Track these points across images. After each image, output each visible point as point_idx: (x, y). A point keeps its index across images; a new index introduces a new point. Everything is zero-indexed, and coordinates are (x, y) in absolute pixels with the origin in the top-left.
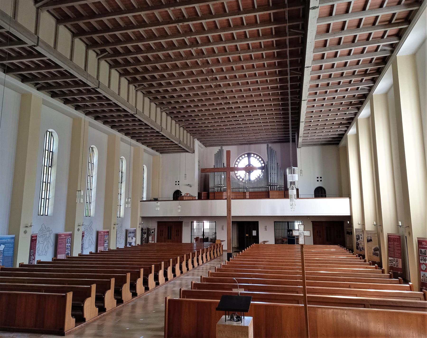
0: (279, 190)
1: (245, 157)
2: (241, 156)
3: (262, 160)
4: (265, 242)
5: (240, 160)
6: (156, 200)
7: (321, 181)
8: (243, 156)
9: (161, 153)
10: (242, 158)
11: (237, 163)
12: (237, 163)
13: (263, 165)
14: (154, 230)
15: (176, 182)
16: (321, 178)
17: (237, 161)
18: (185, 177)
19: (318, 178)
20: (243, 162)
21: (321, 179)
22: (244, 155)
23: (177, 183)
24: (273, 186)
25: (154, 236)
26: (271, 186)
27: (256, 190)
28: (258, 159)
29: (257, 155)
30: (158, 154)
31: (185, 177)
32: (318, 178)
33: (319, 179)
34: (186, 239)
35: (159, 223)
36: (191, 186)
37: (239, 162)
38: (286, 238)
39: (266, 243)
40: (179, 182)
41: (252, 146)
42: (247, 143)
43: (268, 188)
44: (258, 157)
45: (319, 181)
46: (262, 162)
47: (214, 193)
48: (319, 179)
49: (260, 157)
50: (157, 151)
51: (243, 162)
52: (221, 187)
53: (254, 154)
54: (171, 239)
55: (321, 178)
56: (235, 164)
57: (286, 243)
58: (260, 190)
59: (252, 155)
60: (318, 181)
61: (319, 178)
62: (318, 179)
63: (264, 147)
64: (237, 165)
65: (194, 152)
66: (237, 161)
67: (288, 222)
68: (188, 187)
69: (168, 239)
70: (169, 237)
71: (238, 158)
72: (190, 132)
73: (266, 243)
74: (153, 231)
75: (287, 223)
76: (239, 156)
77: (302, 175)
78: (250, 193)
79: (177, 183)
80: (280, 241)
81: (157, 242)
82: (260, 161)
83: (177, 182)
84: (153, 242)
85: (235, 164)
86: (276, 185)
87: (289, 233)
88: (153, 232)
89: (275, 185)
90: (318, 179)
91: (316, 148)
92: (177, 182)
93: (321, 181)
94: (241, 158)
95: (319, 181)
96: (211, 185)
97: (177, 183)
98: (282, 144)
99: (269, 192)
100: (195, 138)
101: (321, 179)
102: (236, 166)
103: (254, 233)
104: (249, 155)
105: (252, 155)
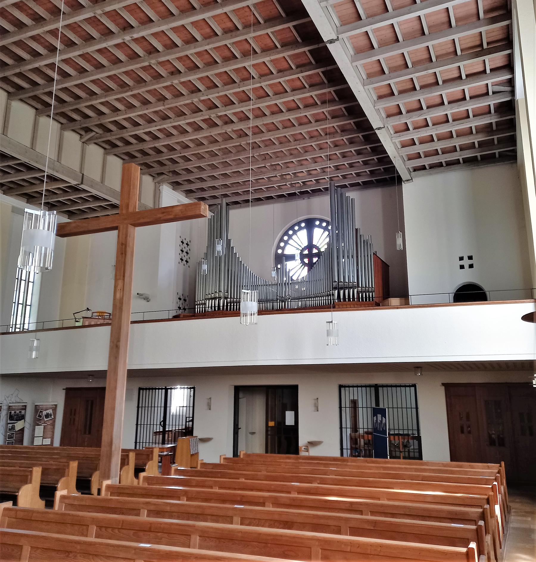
4: (312, 444)
7: (471, 266)
16: (470, 258)
21: (470, 262)
25: (53, 425)
32: (461, 259)
33: (466, 262)
35: (70, 393)
36: (147, 299)
45: (466, 266)
48: (466, 262)
60: (462, 267)
61: (466, 258)
62: (462, 263)
67: (376, 387)
74: (50, 411)
75: (373, 389)
84: (47, 442)
88: (47, 416)
90: (462, 263)
93: (471, 266)
95: (466, 266)
101: (470, 262)
103: (289, 419)
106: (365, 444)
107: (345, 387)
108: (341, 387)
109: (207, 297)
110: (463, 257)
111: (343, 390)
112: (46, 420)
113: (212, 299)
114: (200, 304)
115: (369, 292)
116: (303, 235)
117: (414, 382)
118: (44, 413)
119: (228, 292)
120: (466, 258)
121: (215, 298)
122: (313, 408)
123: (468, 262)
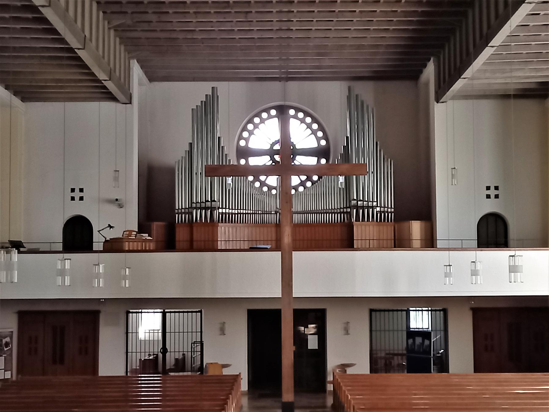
0: (381, 219)
1: (270, 117)
2: (258, 115)
3: (321, 128)
4: (343, 367)
5: (256, 126)
6: (17, 245)
7: (497, 196)
8: (264, 115)
9: (23, 100)
10: (262, 121)
11: (245, 134)
12: (245, 134)
13: (323, 143)
14: (11, 338)
15: (73, 190)
16: (496, 188)
17: (245, 129)
18: (116, 179)
19: (488, 188)
20: (264, 134)
21: (496, 192)
22: (267, 110)
23: (77, 194)
24: (363, 207)
25: (11, 355)
26: (357, 207)
27: (311, 218)
28: (309, 126)
29: (307, 114)
30: (16, 101)
31: (116, 179)
32: (488, 188)
33: (492, 192)
34: (111, 363)
36: (121, 206)
37: (251, 133)
38: (402, 355)
39: (349, 371)
40: (81, 190)
41: (292, 85)
42: (280, 76)
43: (350, 214)
44: (308, 120)
45: (493, 196)
46: (320, 134)
47: (191, 224)
48: (492, 192)
49: (315, 120)
50: (16, 94)
51: (264, 134)
52: (212, 209)
53: (298, 110)
54: (62, 361)
55: (496, 188)
56: (240, 138)
57: (400, 368)
58: (328, 218)
59: (292, 112)
60: (488, 197)
61: (492, 188)
62: (488, 192)
63: (333, 93)
64: (247, 140)
65: (130, 102)
66: (245, 129)
68: (113, 208)
69: (54, 362)
70: (58, 358)
71: (251, 121)
72: (124, 41)
73: (349, 371)
74: (8, 339)
76: (255, 113)
77: (455, 182)
78: (296, 227)
79: (77, 195)
80: (381, 363)
81: (19, 372)
82: (314, 132)
83: (77, 190)
85: (240, 138)
86: (372, 207)
87: (411, 341)
88: (7, 344)
89: (368, 207)
90: (488, 192)
91: (486, 105)
92: (77, 190)
93: (497, 196)
94: (257, 120)
95: (493, 196)
96: (181, 201)
97: (77, 195)
98: (381, 84)
99: (350, 227)
100: (133, 58)
101: (496, 192)
102: (242, 143)
104: (282, 111)
105: (292, 112)
106: (380, 363)
107: (376, 311)
108: (371, 311)
109: (194, 205)
110: (490, 187)
111: (373, 313)
112: (5, 349)
113: (201, 208)
114: (182, 213)
115: (387, 212)
116: (311, 143)
117: (445, 307)
118: (4, 341)
119: (219, 201)
120: (492, 188)
121: (206, 209)
122: (343, 332)
123: (493, 192)
